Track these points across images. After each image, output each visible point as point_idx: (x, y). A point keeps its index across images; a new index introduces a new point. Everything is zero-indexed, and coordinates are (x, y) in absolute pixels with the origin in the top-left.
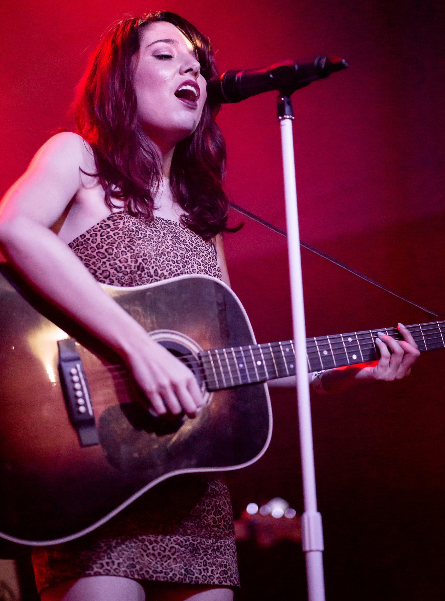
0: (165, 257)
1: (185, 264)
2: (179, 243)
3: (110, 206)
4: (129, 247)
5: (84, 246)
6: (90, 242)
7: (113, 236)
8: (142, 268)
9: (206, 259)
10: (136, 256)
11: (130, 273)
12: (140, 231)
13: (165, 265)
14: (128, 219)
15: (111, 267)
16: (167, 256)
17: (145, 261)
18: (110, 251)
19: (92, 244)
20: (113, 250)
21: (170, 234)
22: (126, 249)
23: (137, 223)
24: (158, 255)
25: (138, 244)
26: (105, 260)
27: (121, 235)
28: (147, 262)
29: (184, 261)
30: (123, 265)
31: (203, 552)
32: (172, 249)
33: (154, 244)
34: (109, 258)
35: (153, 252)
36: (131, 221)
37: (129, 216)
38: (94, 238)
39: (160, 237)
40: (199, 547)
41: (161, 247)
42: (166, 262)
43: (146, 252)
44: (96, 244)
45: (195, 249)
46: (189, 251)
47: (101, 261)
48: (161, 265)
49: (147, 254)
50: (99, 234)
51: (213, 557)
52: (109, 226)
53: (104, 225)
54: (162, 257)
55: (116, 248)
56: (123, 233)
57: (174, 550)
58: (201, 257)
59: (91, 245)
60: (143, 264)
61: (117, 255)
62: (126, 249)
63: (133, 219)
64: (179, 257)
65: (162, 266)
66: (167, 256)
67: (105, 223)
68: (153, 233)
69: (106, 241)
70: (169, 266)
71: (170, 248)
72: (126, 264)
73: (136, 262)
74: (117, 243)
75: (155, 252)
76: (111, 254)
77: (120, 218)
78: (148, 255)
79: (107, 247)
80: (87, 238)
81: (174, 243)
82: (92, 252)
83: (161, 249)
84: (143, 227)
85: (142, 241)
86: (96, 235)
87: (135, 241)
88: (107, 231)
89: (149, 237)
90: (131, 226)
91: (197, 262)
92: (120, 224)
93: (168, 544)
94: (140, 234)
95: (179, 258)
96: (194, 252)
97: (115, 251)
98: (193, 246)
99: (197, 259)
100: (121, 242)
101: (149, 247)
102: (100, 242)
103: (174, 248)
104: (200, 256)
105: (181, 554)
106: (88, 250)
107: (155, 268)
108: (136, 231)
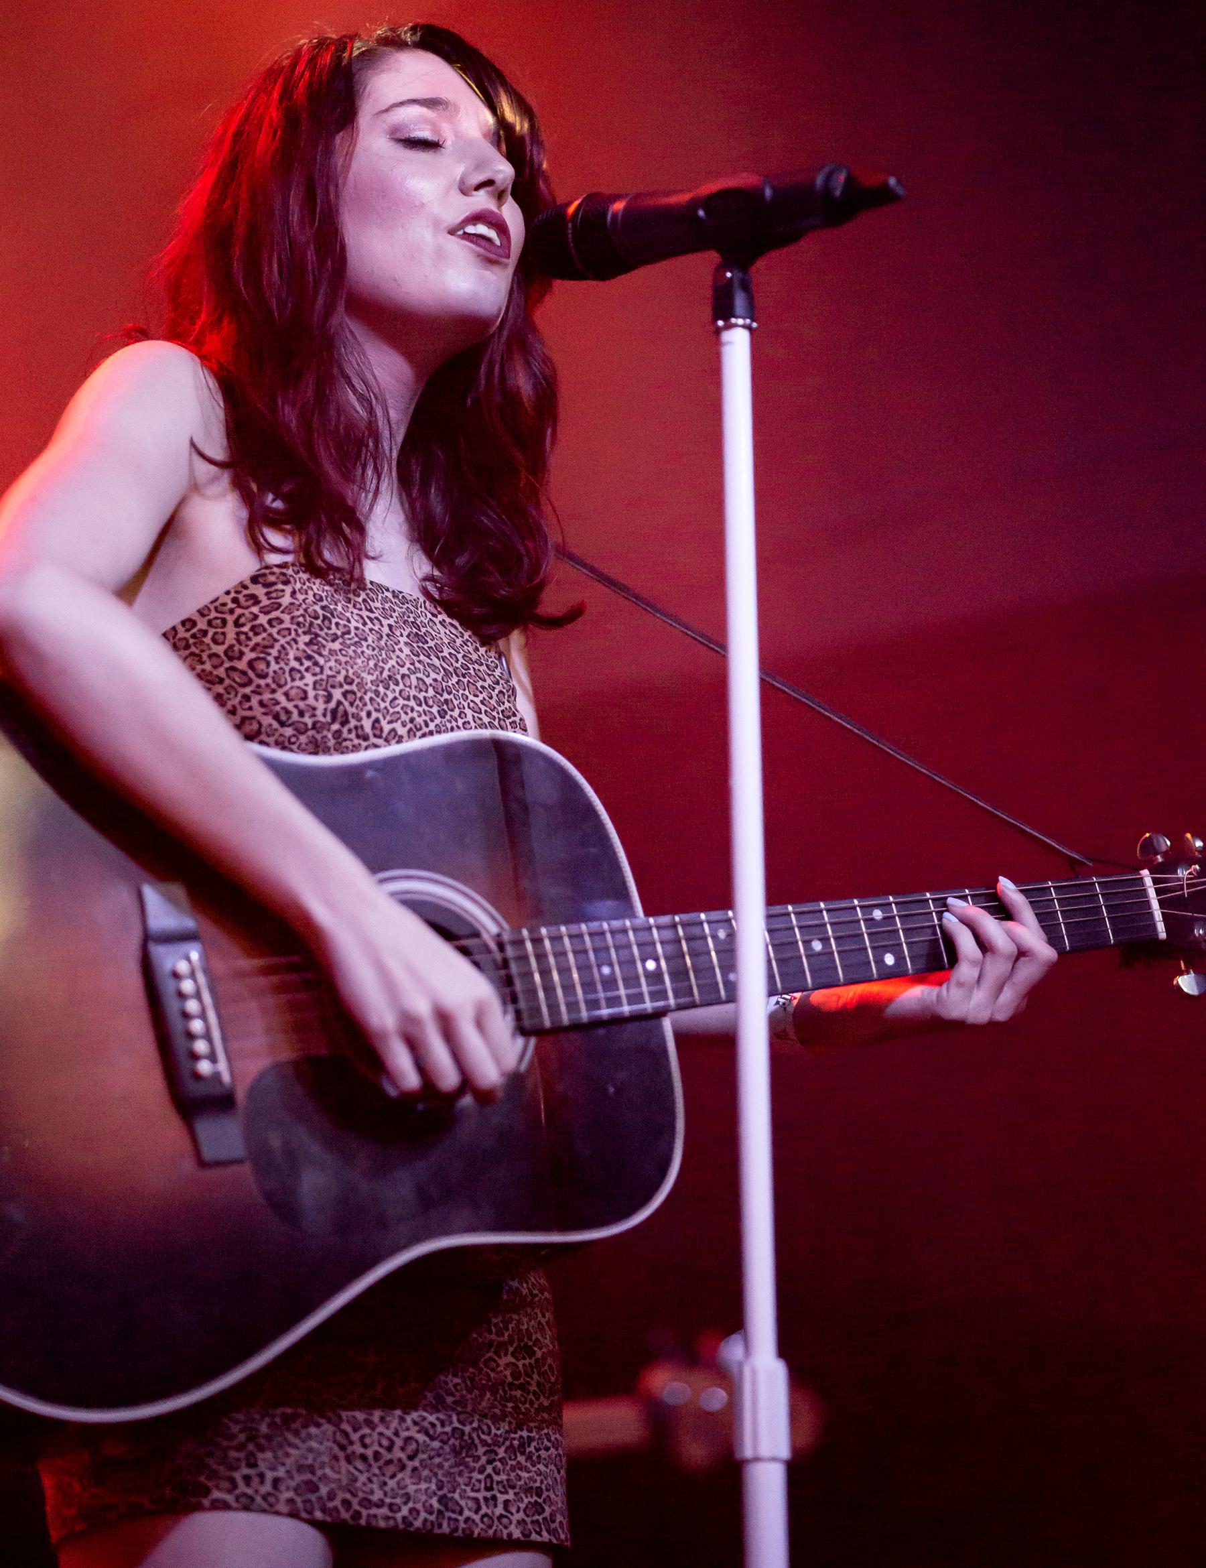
0: (398, 689)
1: (445, 707)
2: (426, 653)
3: (258, 547)
4: (309, 658)
5: (193, 649)
6: (207, 640)
7: (267, 626)
8: (342, 716)
9: (491, 698)
10: (327, 683)
11: (314, 727)
12: (334, 617)
13: (398, 709)
14: (304, 584)
15: (263, 710)
16: (401, 686)
17: (350, 696)
18: (261, 666)
19: (212, 645)
20: (268, 664)
21: (404, 630)
22: (302, 664)
23: (326, 597)
24: (382, 682)
25: (330, 650)
26: (247, 690)
27: (287, 625)
28: (355, 700)
29: (442, 699)
30: (296, 707)
31: (485, 1454)
32: (412, 667)
33: (369, 652)
34: (259, 686)
35: (369, 673)
36: (312, 589)
37: (305, 576)
38: (219, 630)
39: (382, 636)
40: (477, 1441)
41: (385, 661)
42: (401, 701)
43: (350, 674)
44: (225, 646)
45: (464, 671)
46: (452, 676)
47: (237, 693)
48: (389, 708)
49: (355, 678)
50: (230, 619)
51: (508, 1468)
52: (255, 599)
53: (244, 596)
54: (391, 688)
55: (277, 659)
56: (293, 618)
57: (414, 1446)
58: (481, 693)
59: (210, 649)
60: (346, 704)
61: (280, 679)
62: (302, 664)
63: (317, 586)
64: (430, 689)
65: (391, 711)
66: (401, 686)
67: (245, 592)
68: (365, 624)
69: (249, 639)
70: (409, 712)
71: (408, 665)
72: (302, 704)
73: (329, 698)
74: (277, 646)
75: (372, 675)
76: (263, 676)
77: (283, 578)
78: (357, 681)
79: (253, 655)
80: (200, 630)
81: (415, 652)
82: (215, 667)
83: (387, 667)
84: (339, 608)
85: (341, 644)
86: (224, 622)
87: (324, 642)
88: (251, 613)
89: (356, 634)
90: (311, 602)
91: (472, 705)
92: (283, 596)
93: (399, 1429)
94: (333, 626)
95: (431, 692)
96: (462, 679)
97: (274, 666)
98: (460, 663)
99: (471, 697)
100: (288, 643)
101: (359, 661)
102: (234, 642)
103: (417, 665)
104: (477, 688)
105: (431, 1458)
106: (203, 663)
107: (374, 715)
108: (325, 617)
